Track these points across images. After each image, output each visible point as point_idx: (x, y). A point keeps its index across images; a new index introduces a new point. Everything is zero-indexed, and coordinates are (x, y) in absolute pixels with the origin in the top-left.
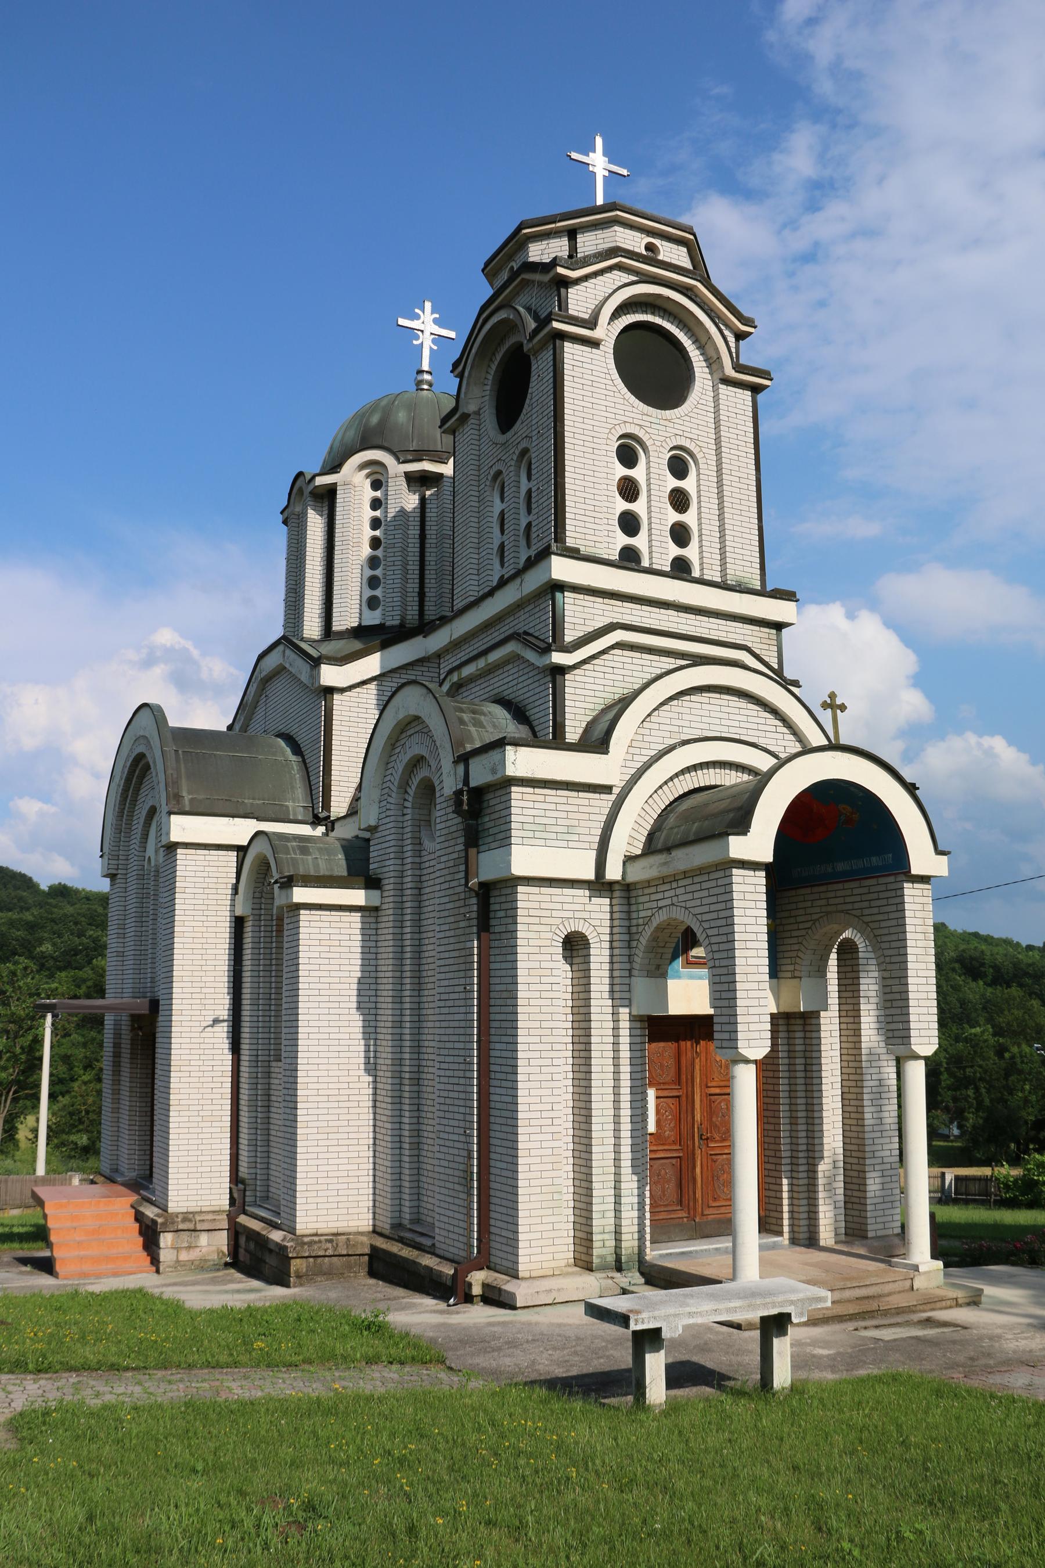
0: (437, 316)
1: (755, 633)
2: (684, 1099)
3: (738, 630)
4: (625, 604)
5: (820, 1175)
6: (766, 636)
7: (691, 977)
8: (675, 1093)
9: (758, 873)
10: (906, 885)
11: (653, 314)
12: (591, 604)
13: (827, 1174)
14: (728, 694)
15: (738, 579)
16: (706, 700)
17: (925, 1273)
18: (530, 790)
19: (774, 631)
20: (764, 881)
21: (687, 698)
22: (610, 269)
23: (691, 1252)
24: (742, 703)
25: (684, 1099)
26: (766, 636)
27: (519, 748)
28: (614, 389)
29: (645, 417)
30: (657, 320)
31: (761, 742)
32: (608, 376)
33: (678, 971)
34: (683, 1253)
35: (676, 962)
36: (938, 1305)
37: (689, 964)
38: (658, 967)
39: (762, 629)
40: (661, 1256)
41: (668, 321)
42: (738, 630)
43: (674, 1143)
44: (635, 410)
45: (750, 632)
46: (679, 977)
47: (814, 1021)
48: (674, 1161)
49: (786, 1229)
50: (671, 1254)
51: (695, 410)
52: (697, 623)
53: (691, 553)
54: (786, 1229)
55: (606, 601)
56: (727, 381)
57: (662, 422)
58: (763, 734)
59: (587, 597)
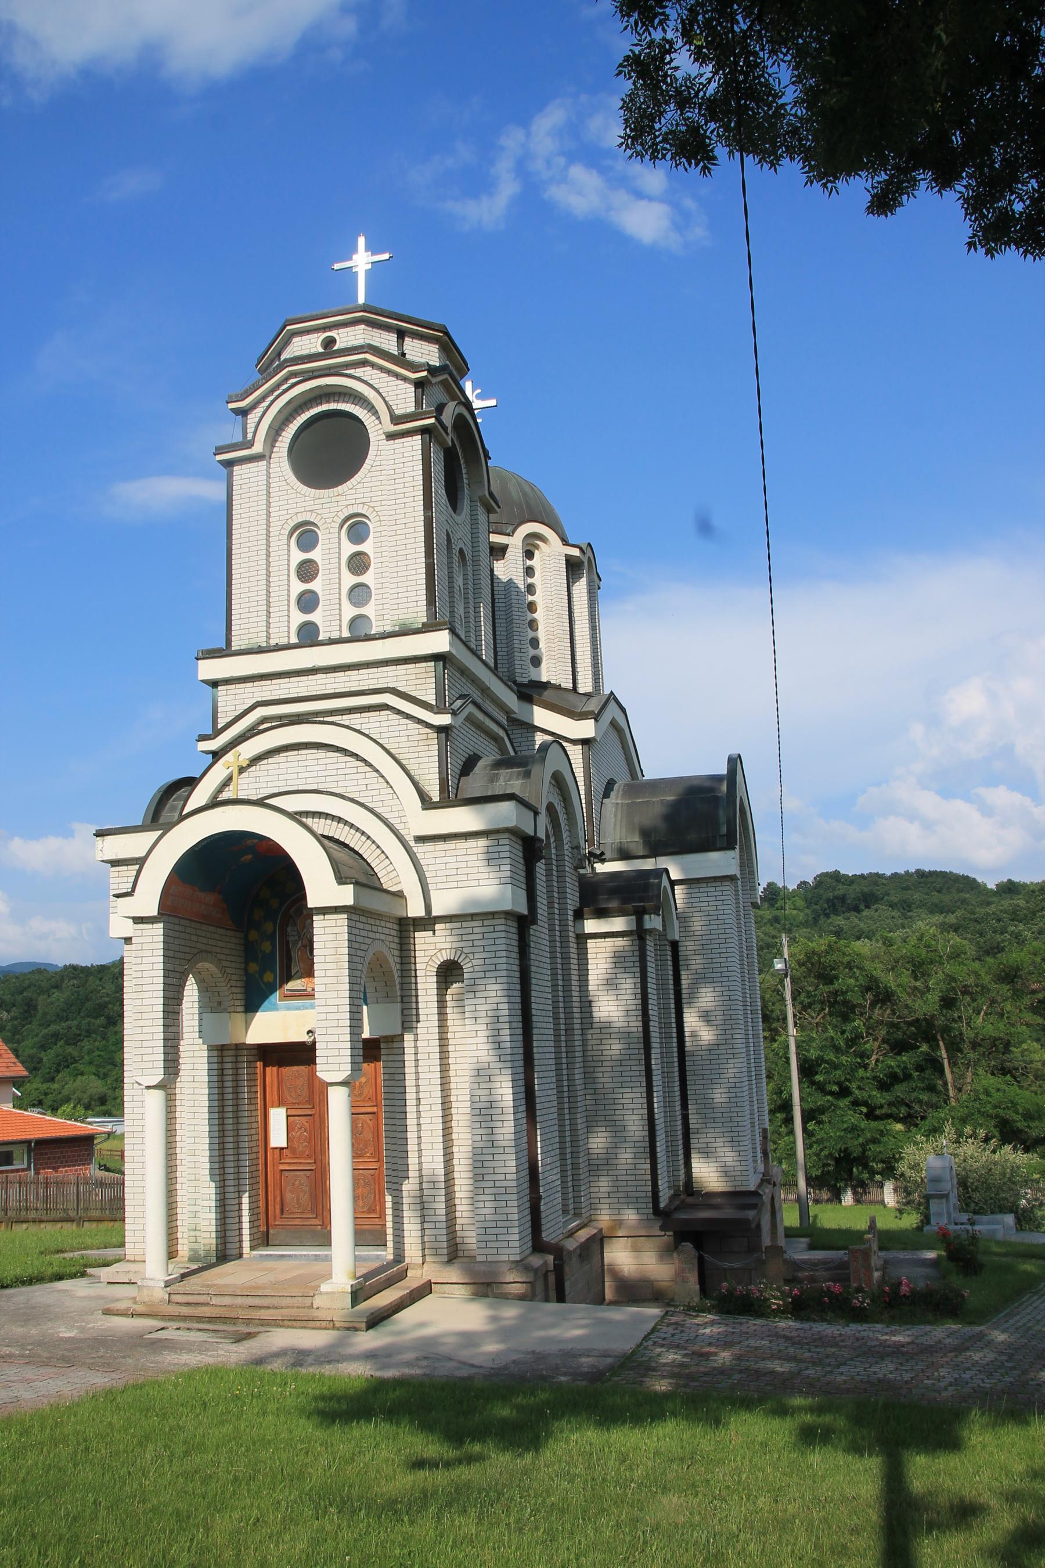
0: (479, 391)
1: (409, 672)
2: (317, 1117)
3: (390, 674)
4: (274, 682)
5: (405, 1194)
6: (423, 670)
7: (288, 1008)
8: (309, 1112)
9: (155, 926)
10: (315, 918)
11: (328, 402)
12: (242, 691)
13: (412, 1194)
14: (306, 748)
15: (402, 622)
16: (284, 759)
17: (327, 1293)
18: (124, 868)
19: (433, 663)
20: (161, 932)
21: (265, 761)
22: (286, 379)
23: (290, 1256)
24: (321, 754)
25: (317, 1117)
26: (423, 670)
27: (106, 838)
28: (288, 487)
29: (316, 502)
30: (333, 406)
31: (321, 787)
32: (282, 479)
33: (275, 1004)
34: (282, 1256)
35: (273, 995)
36: (311, 1324)
37: (286, 997)
38: (220, 1003)
39: (418, 665)
40: (261, 1256)
41: (344, 402)
42: (390, 674)
43: (309, 1157)
44: (307, 499)
45: (404, 672)
46: (277, 1010)
47: (396, 1045)
48: (308, 1173)
49: (390, 1244)
50: (271, 1255)
51: (370, 474)
52: (347, 679)
53: (369, 610)
54: (390, 1244)
55: (256, 684)
56: (391, 436)
57: (334, 499)
58: (323, 779)
59: (238, 686)
